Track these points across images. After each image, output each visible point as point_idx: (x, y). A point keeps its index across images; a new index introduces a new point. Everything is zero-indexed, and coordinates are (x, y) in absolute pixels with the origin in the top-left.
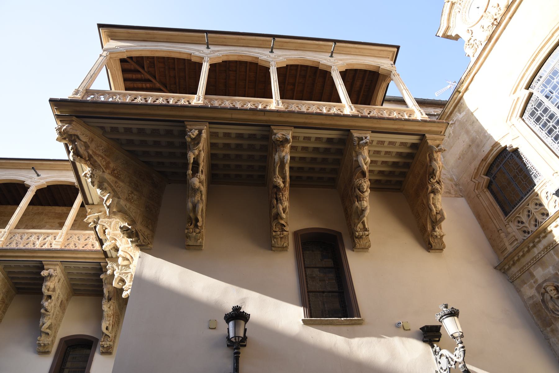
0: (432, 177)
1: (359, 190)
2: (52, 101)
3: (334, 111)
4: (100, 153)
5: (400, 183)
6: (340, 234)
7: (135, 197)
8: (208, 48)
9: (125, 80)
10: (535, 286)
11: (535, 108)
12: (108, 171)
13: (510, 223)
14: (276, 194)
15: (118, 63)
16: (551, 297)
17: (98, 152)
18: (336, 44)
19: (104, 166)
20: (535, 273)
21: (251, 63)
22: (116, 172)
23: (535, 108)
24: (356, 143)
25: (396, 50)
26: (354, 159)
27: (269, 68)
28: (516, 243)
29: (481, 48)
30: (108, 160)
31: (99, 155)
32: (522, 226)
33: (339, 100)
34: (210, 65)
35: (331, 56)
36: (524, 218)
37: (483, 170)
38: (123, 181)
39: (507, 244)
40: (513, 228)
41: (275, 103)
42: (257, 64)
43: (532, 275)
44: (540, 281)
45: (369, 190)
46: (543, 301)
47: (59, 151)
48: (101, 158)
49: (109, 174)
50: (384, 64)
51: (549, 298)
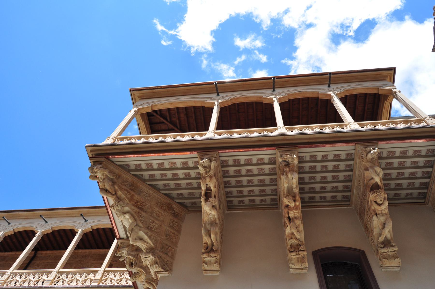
1: (376, 202)
3: (337, 129)
4: (125, 188)
5: (424, 196)
7: (157, 226)
8: (218, 95)
12: (132, 202)
14: (288, 213)
15: (146, 117)
17: (123, 187)
19: (128, 198)
22: (139, 204)
25: (393, 71)
27: (273, 104)
30: (132, 193)
31: (125, 190)
34: (220, 108)
35: (329, 86)
48: (126, 192)
49: (133, 205)
50: (384, 86)
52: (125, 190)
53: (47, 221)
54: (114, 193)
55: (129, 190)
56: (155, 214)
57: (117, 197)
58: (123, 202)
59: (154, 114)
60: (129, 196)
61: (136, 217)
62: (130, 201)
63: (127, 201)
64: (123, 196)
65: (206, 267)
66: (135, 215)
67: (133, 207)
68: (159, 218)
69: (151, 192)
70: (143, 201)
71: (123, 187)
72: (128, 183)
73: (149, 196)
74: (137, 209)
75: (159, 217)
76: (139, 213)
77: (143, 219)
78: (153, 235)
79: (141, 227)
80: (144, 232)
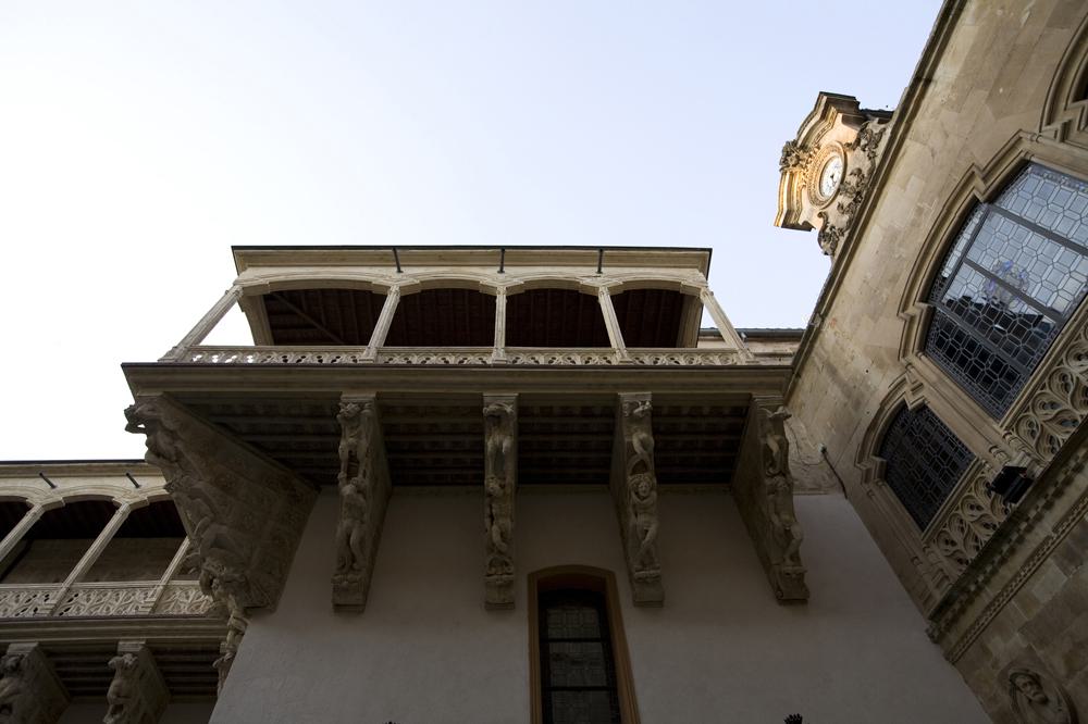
0: (771, 465)
2: (124, 366)
3: (596, 360)
6: (611, 574)
9: (273, 327)
10: (996, 673)
11: (942, 333)
13: (932, 543)
15: (261, 306)
16: (1030, 701)
18: (601, 255)
20: (990, 646)
21: (471, 291)
23: (942, 333)
24: (627, 413)
26: (627, 440)
27: (495, 297)
28: (946, 583)
29: (842, 240)
32: (952, 549)
33: (607, 344)
36: (957, 536)
37: (871, 445)
39: (931, 585)
40: (938, 553)
41: (498, 353)
42: (370, 292)
43: (986, 652)
44: (1003, 664)
45: (654, 494)
46: (1015, 706)
47: (135, 447)
51: (1025, 701)
53: (55, 484)
59: (279, 297)
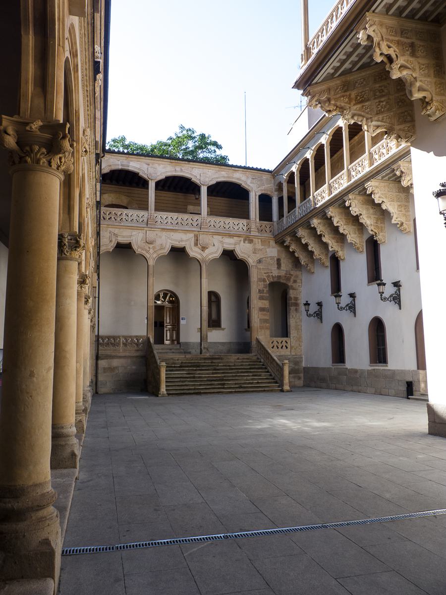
7: (384, 103)
12: (352, 104)
30: (348, 93)
31: (340, 97)
38: (368, 100)
48: (342, 99)
49: (354, 105)
52: (340, 97)
54: (335, 108)
55: (343, 94)
56: (378, 94)
57: (340, 108)
58: (345, 110)
60: (347, 100)
61: (363, 113)
62: (350, 104)
63: (347, 106)
64: (343, 104)
65: (433, 119)
66: (360, 113)
67: (355, 107)
68: (384, 93)
69: (363, 74)
70: (360, 91)
71: (338, 96)
72: (340, 87)
73: (364, 80)
74: (359, 106)
75: (383, 91)
76: (363, 106)
77: (368, 109)
78: (385, 115)
79: (371, 118)
80: (376, 121)
